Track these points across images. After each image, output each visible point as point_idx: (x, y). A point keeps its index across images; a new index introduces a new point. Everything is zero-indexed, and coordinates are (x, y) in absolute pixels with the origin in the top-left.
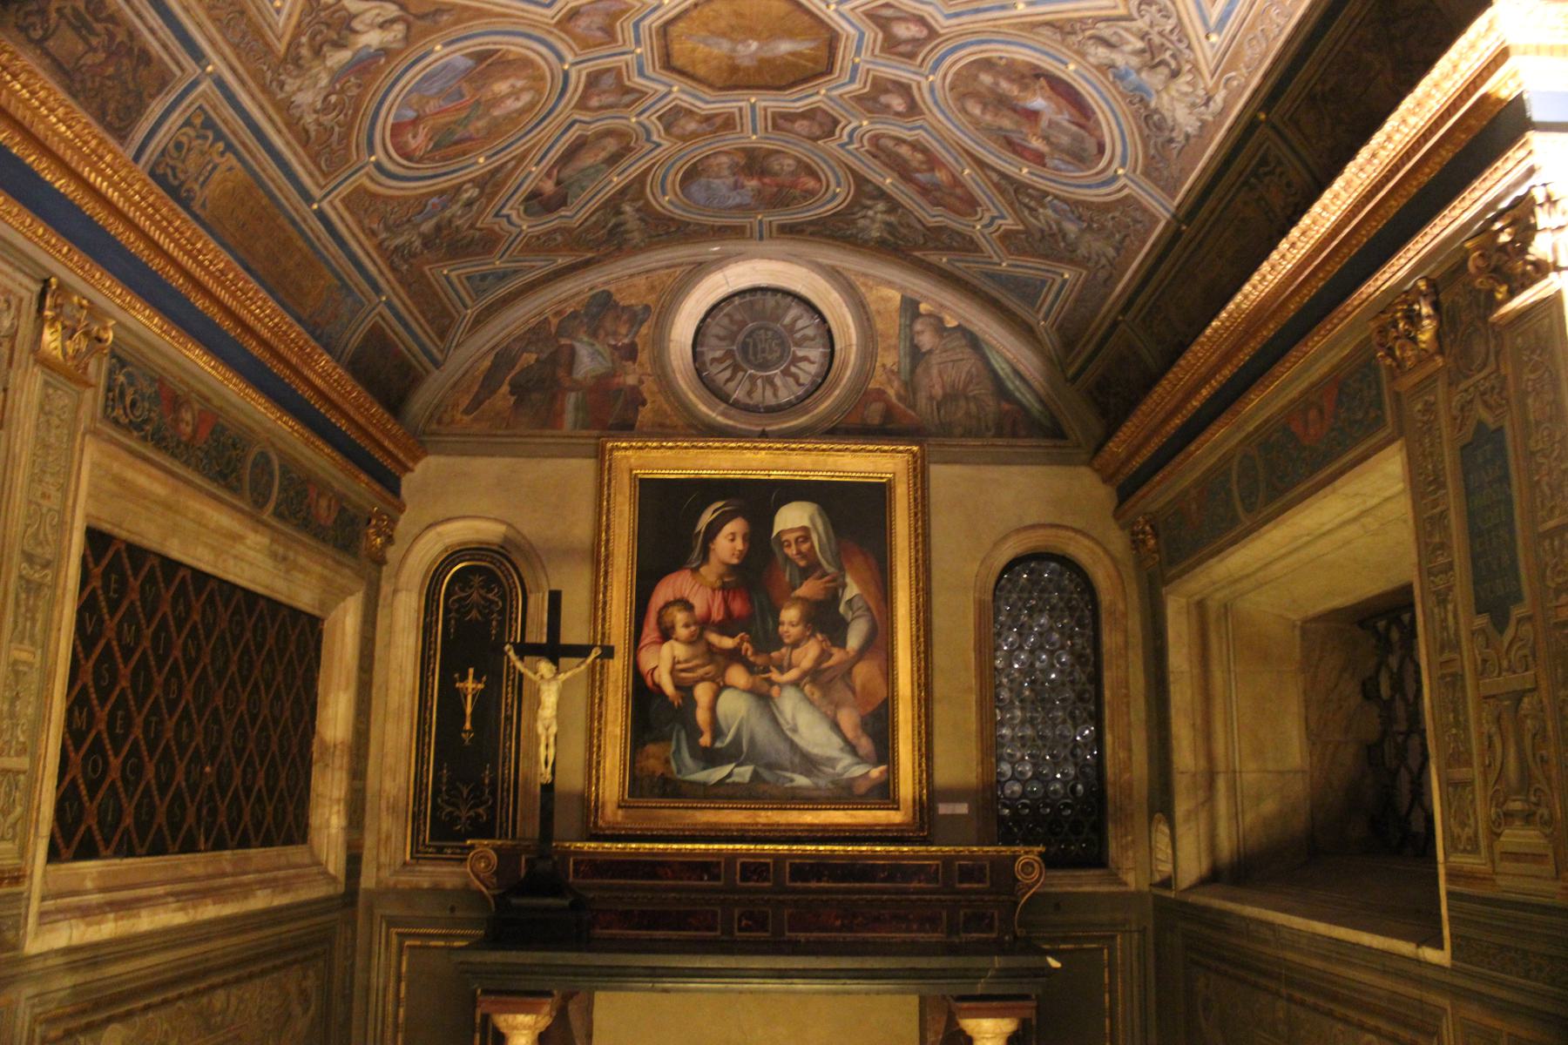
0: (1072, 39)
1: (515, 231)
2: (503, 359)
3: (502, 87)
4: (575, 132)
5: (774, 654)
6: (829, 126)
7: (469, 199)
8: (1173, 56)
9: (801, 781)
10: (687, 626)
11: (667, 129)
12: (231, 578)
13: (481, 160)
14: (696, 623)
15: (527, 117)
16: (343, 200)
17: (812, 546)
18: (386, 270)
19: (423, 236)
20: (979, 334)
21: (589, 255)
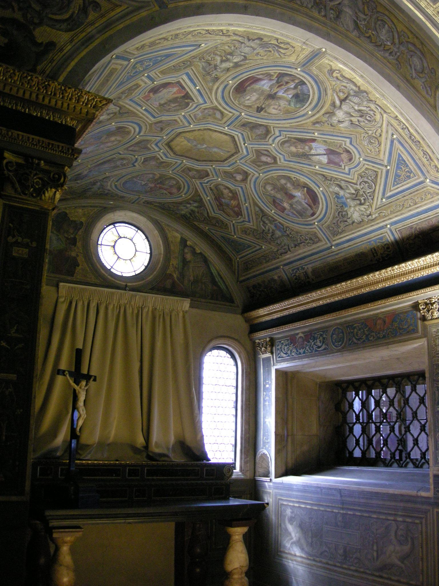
0: (327, 182)
8: (364, 199)
20: (207, 257)
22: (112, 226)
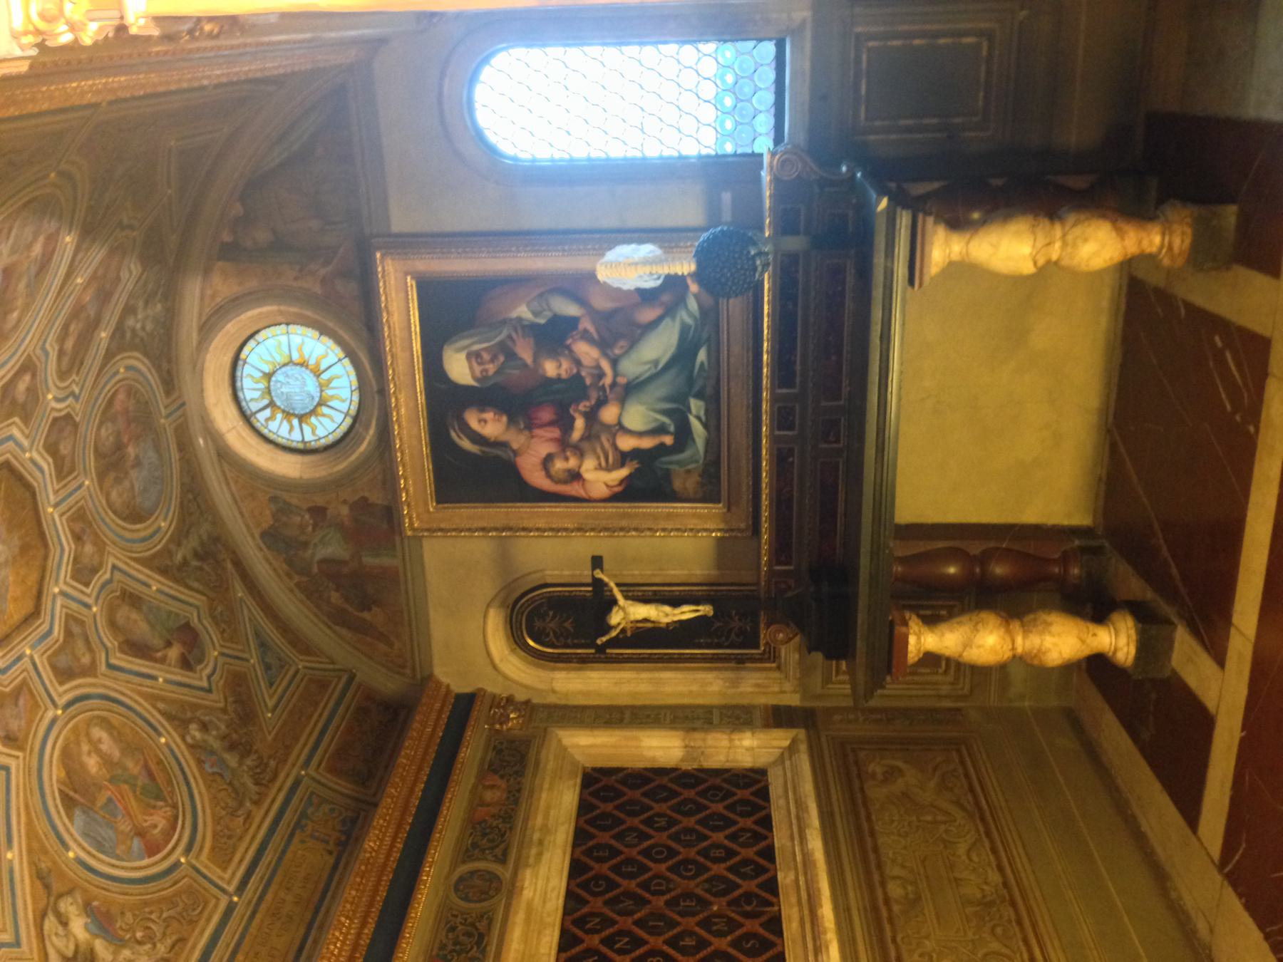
1: (221, 660)
2: (338, 618)
3: (92, 763)
4: (120, 660)
5: (588, 381)
6: (64, 423)
7: (200, 730)
9: (702, 356)
10: (567, 459)
11: (94, 571)
12: (561, 901)
13: (163, 740)
14: (564, 451)
15: (116, 720)
16: (225, 869)
17: (485, 349)
18: (278, 784)
19: (243, 756)
21: (229, 566)
22: (253, 419)
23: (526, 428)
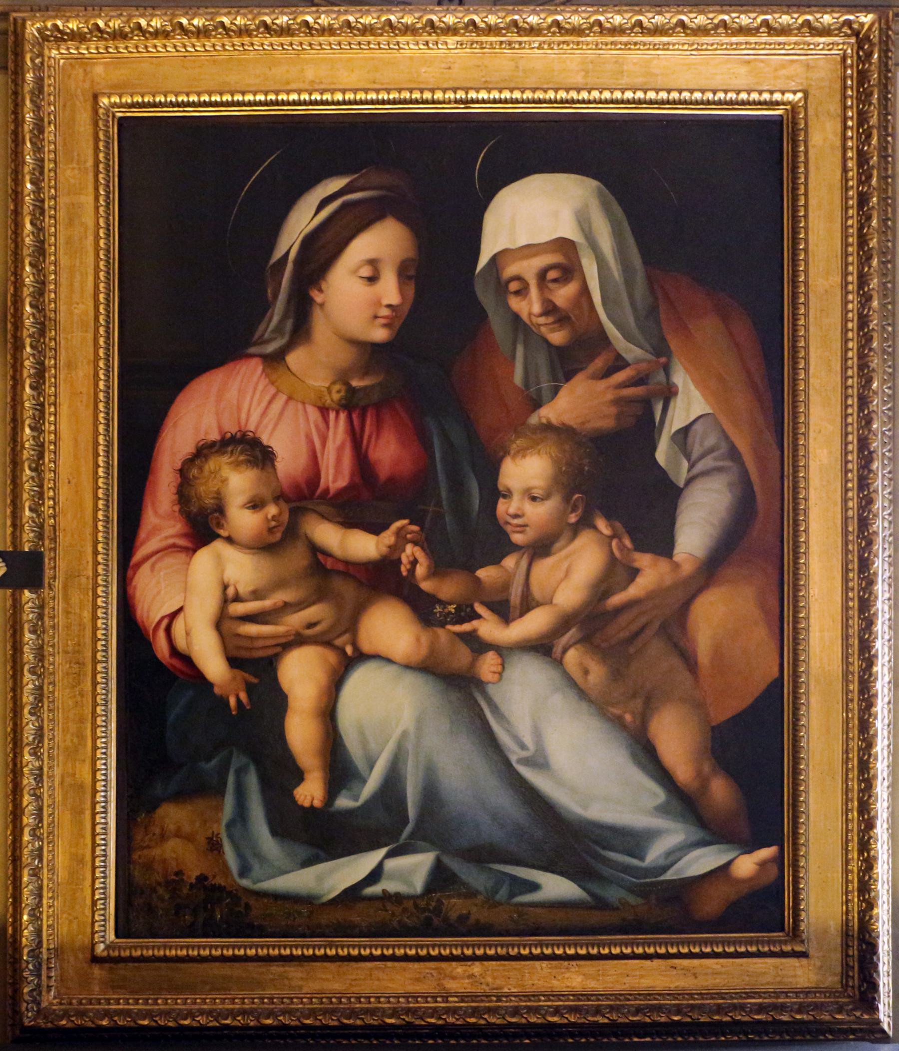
5: (485, 574)
10: (255, 505)
14: (279, 497)
17: (585, 290)
23: (352, 391)
